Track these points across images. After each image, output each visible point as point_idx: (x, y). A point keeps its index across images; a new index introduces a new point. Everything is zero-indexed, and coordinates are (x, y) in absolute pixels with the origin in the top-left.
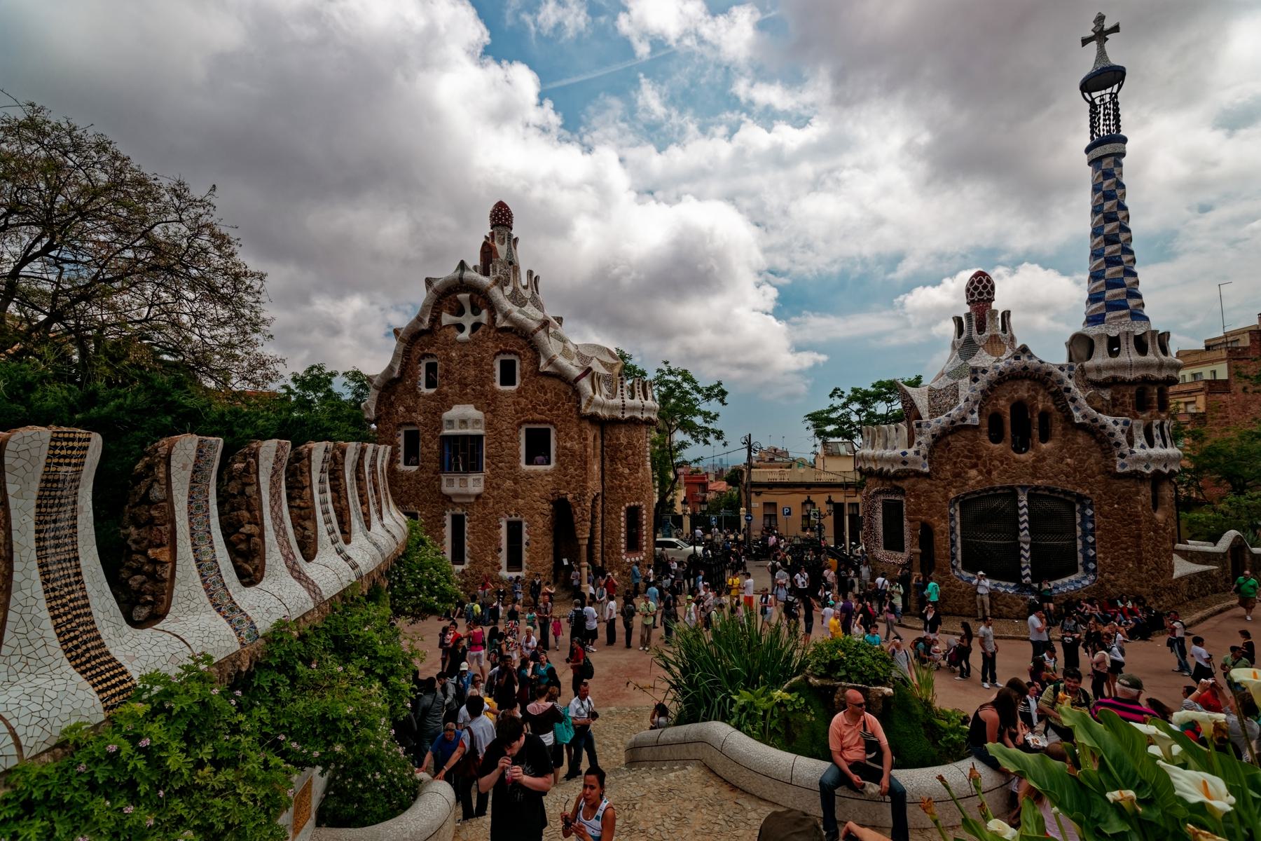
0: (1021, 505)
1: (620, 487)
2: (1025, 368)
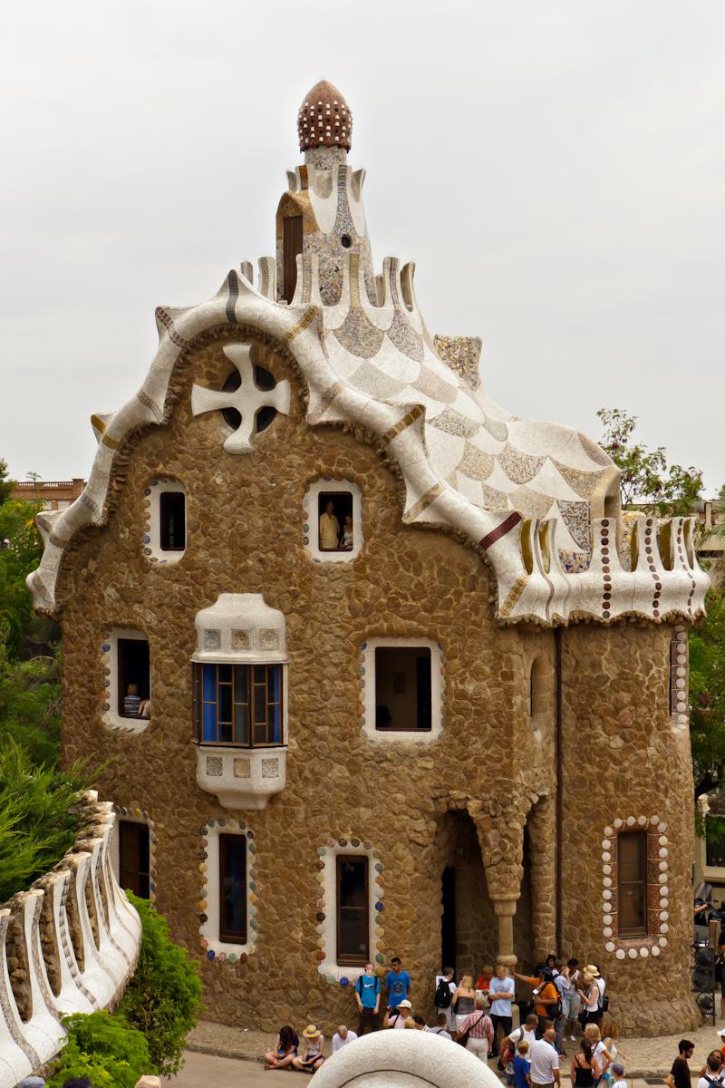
1: (602, 780)
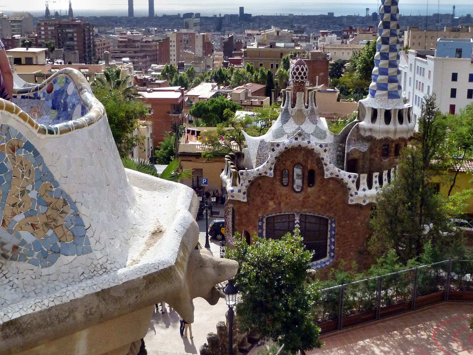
0: (296, 222)
2: (300, 146)
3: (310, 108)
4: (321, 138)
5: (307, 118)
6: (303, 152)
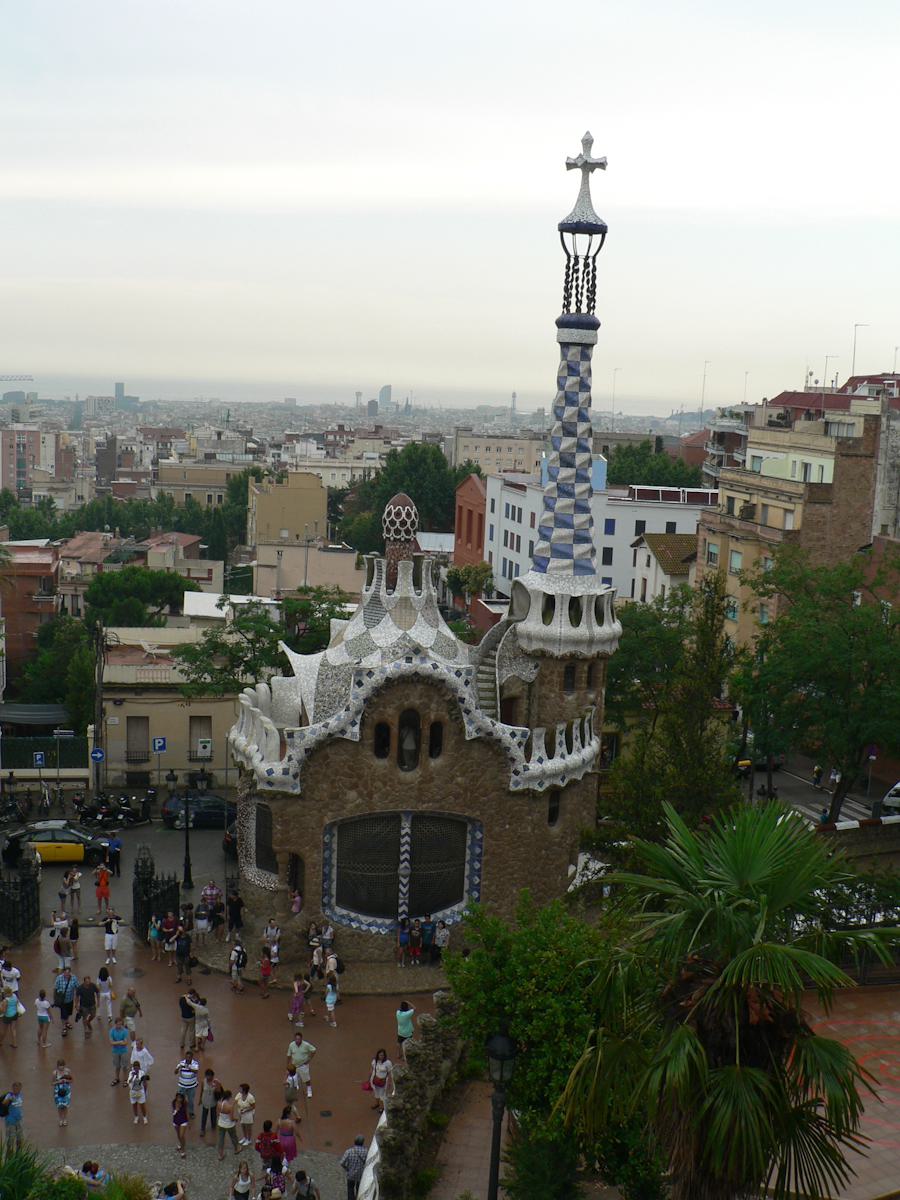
0: (403, 832)
2: (416, 674)
3: (424, 593)
4: (448, 657)
5: (419, 614)
6: (420, 687)
